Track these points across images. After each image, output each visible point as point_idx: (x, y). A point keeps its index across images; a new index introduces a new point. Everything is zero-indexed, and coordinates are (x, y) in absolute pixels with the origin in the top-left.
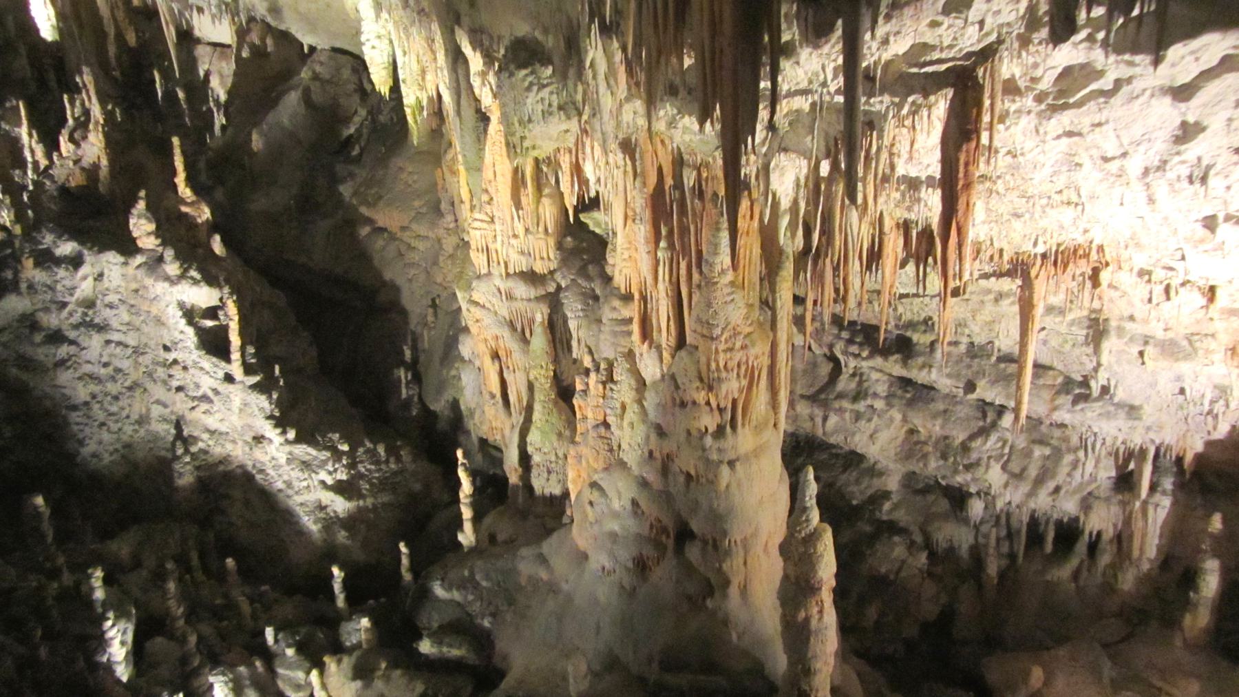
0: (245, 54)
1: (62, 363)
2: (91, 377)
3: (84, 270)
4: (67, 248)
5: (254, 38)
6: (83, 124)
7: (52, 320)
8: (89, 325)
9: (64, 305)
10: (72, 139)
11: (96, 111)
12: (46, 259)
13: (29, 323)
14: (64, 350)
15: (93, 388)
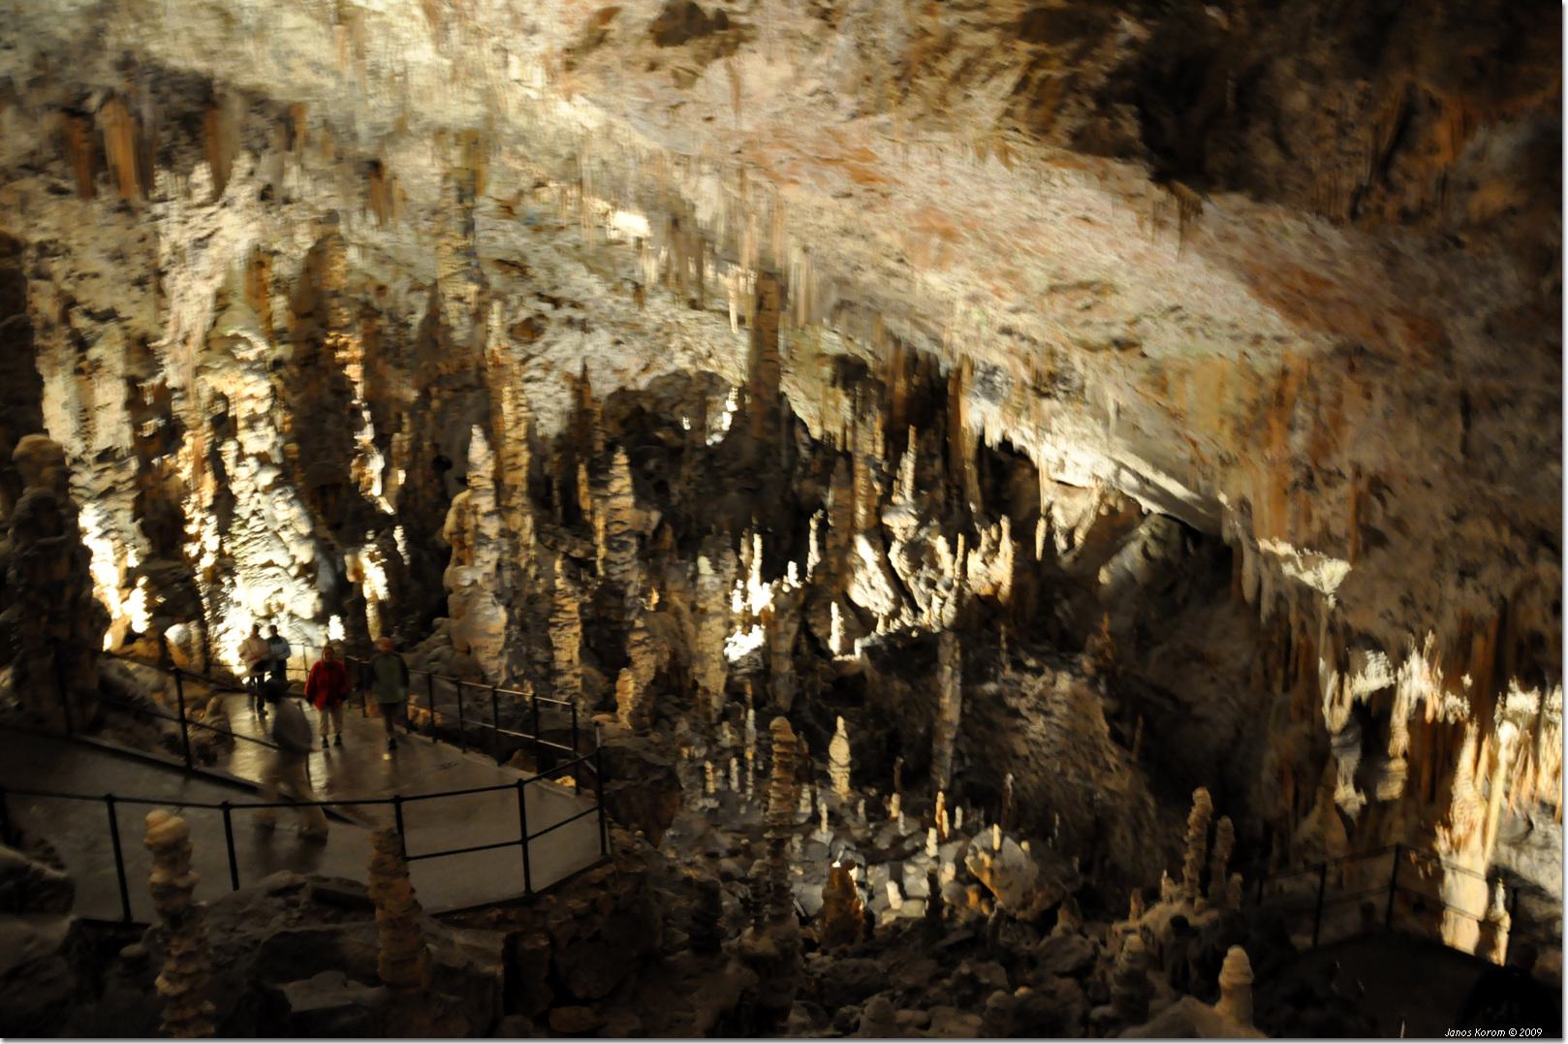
0: (1104, 511)
1: (1018, 730)
2: (1035, 743)
3: (1044, 678)
4: (1032, 663)
5: (1111, 502)
6: (995, 549)
7: (1013, 702)
8: (1037, 710)
9: (1024, 695)
10: (984, 561)
11: (1006, 546)
12: (1019, 666)
13: (998, 699)
14: (1019, 722)
15: (1034, 749)
